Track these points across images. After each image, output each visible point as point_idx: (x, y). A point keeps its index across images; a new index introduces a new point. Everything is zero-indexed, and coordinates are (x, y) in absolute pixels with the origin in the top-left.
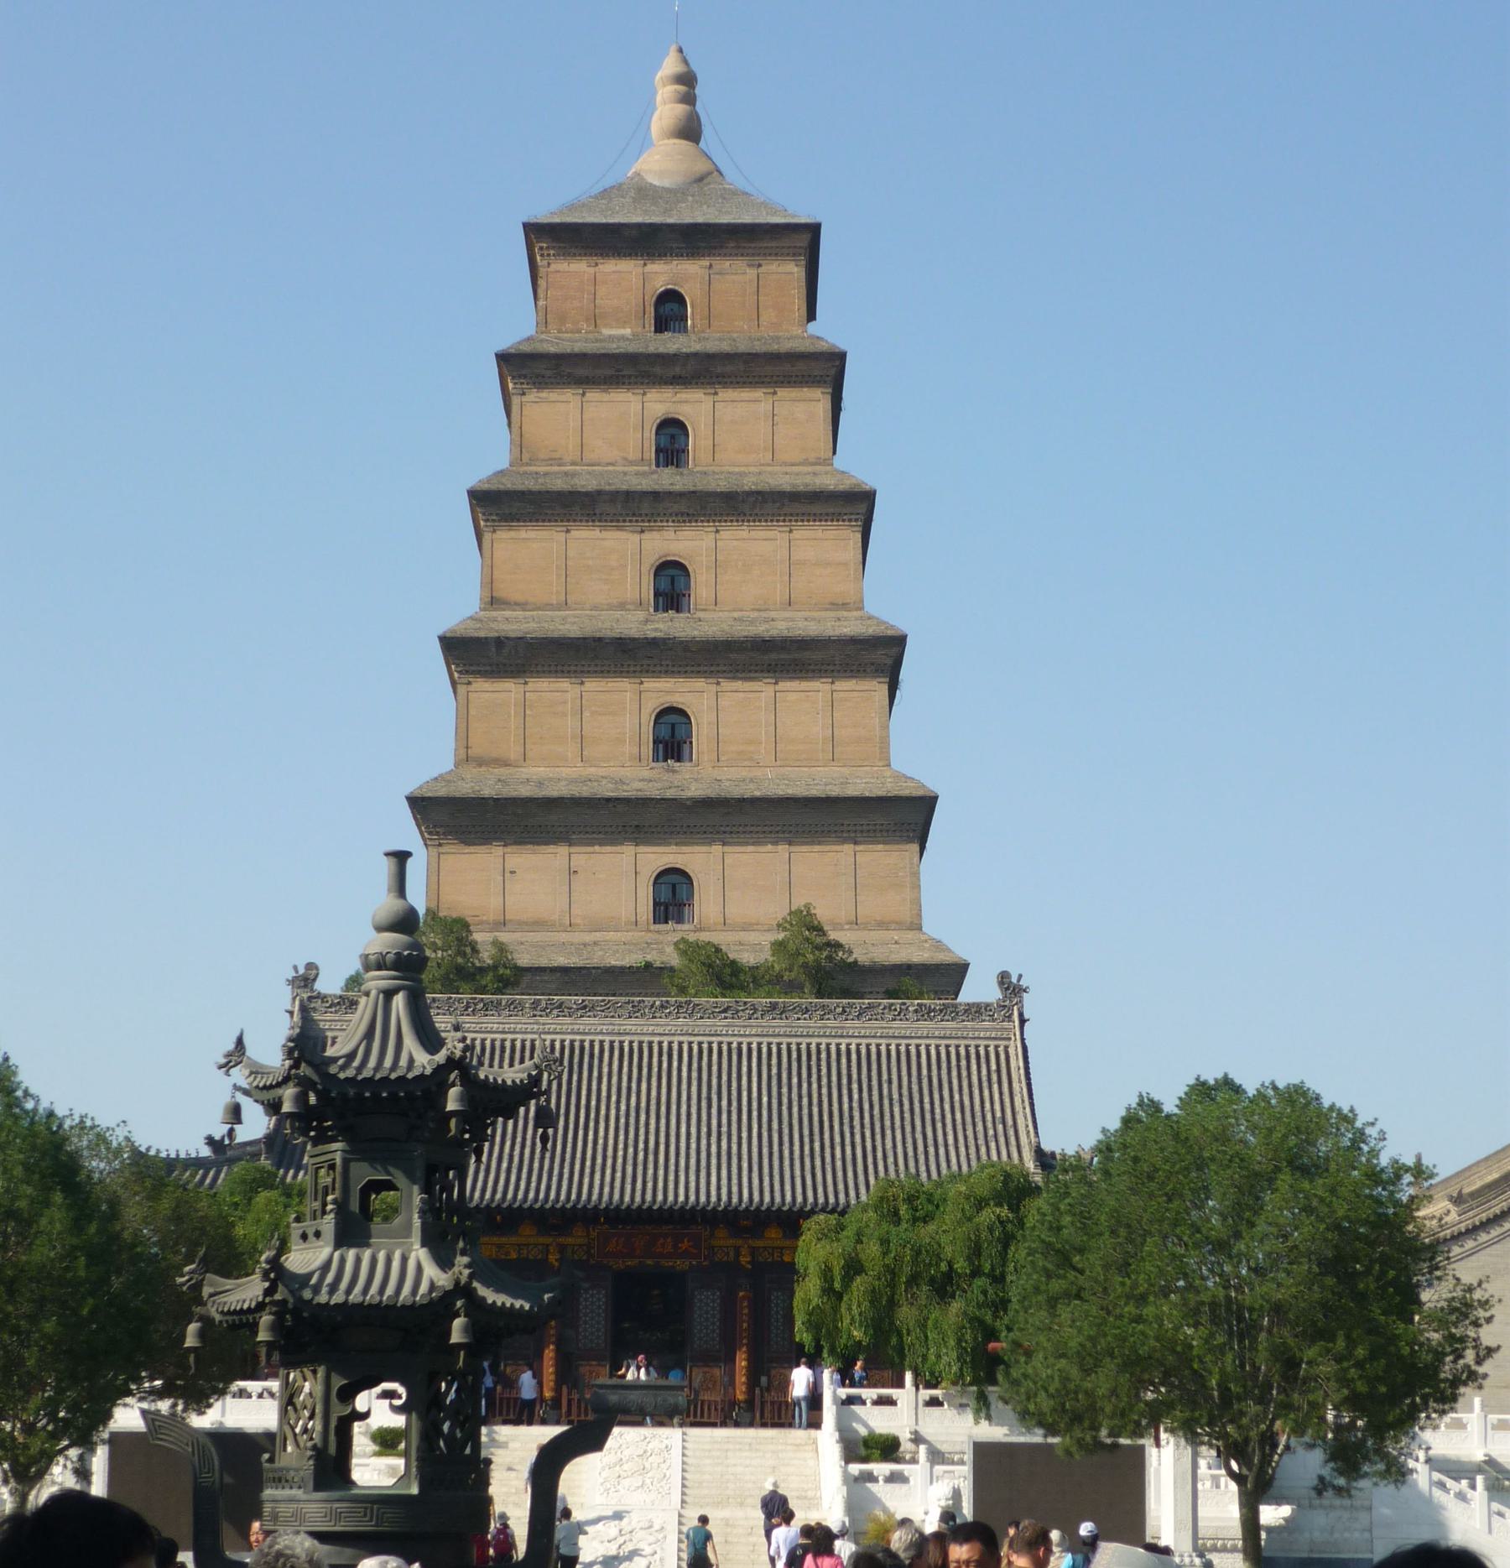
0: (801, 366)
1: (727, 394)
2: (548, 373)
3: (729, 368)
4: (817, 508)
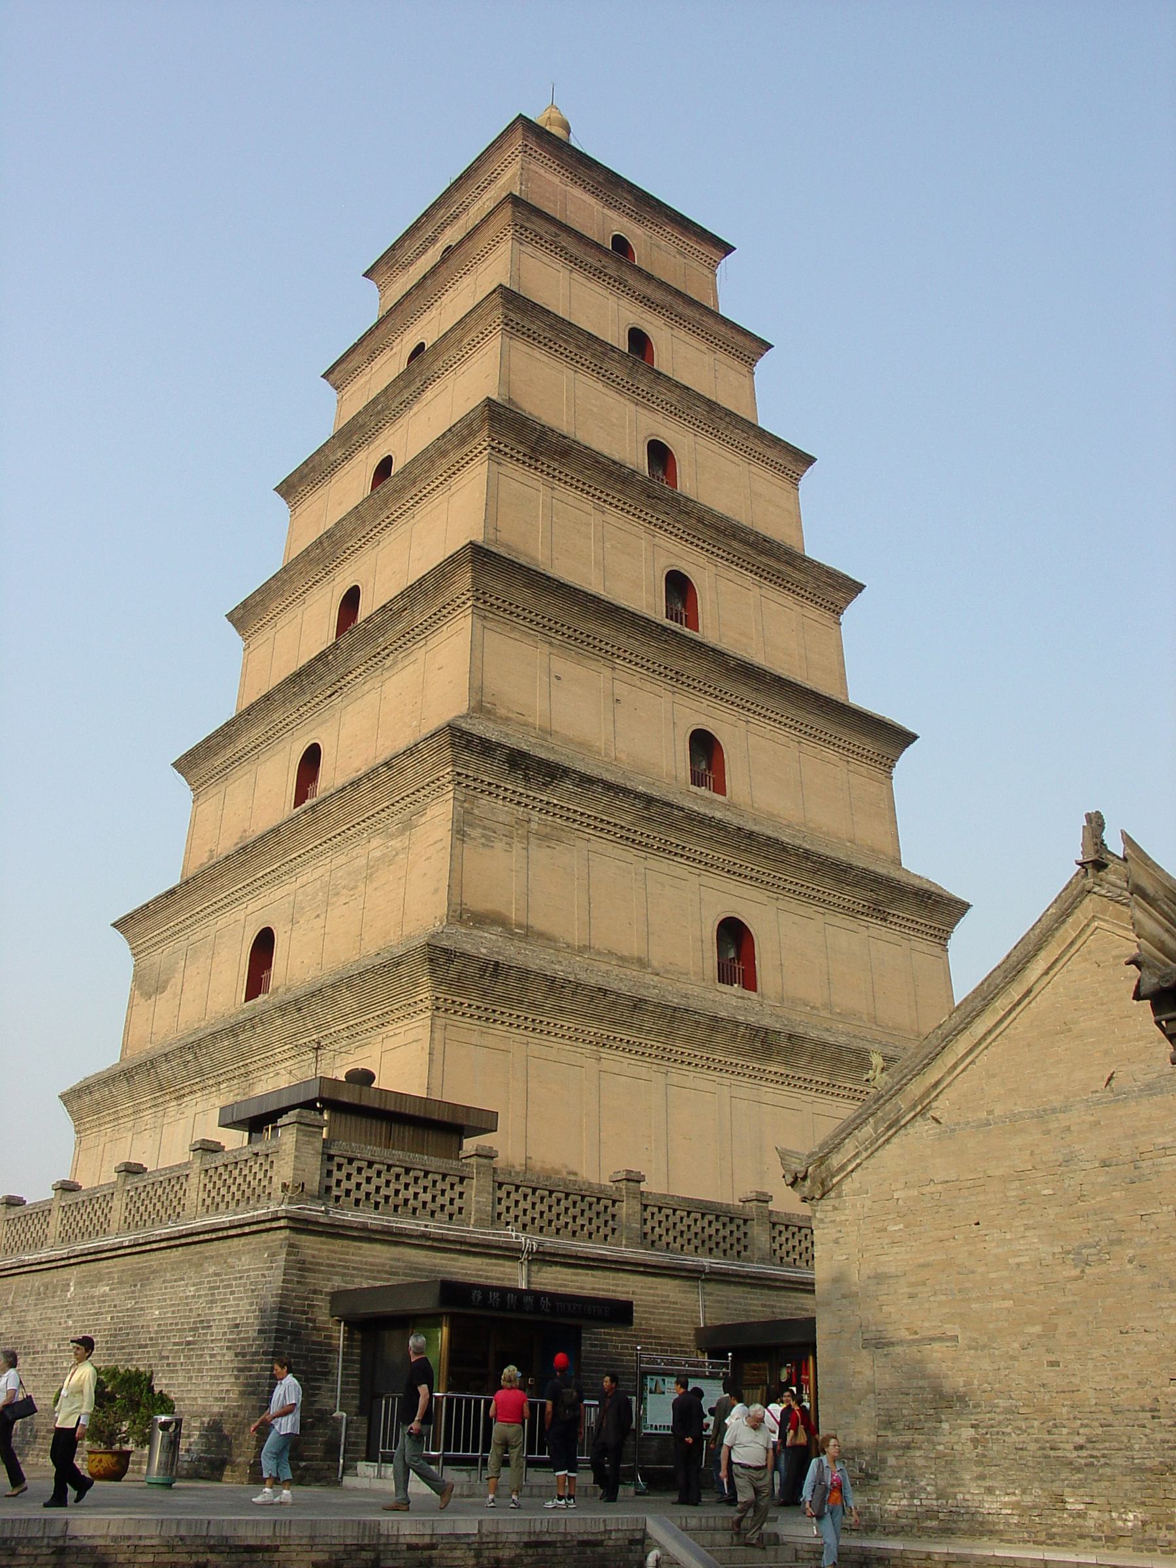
0: (739, 338)
1: (682, 334)
2: (548, 237)
3: (689, 312)
4: (772, 454)
